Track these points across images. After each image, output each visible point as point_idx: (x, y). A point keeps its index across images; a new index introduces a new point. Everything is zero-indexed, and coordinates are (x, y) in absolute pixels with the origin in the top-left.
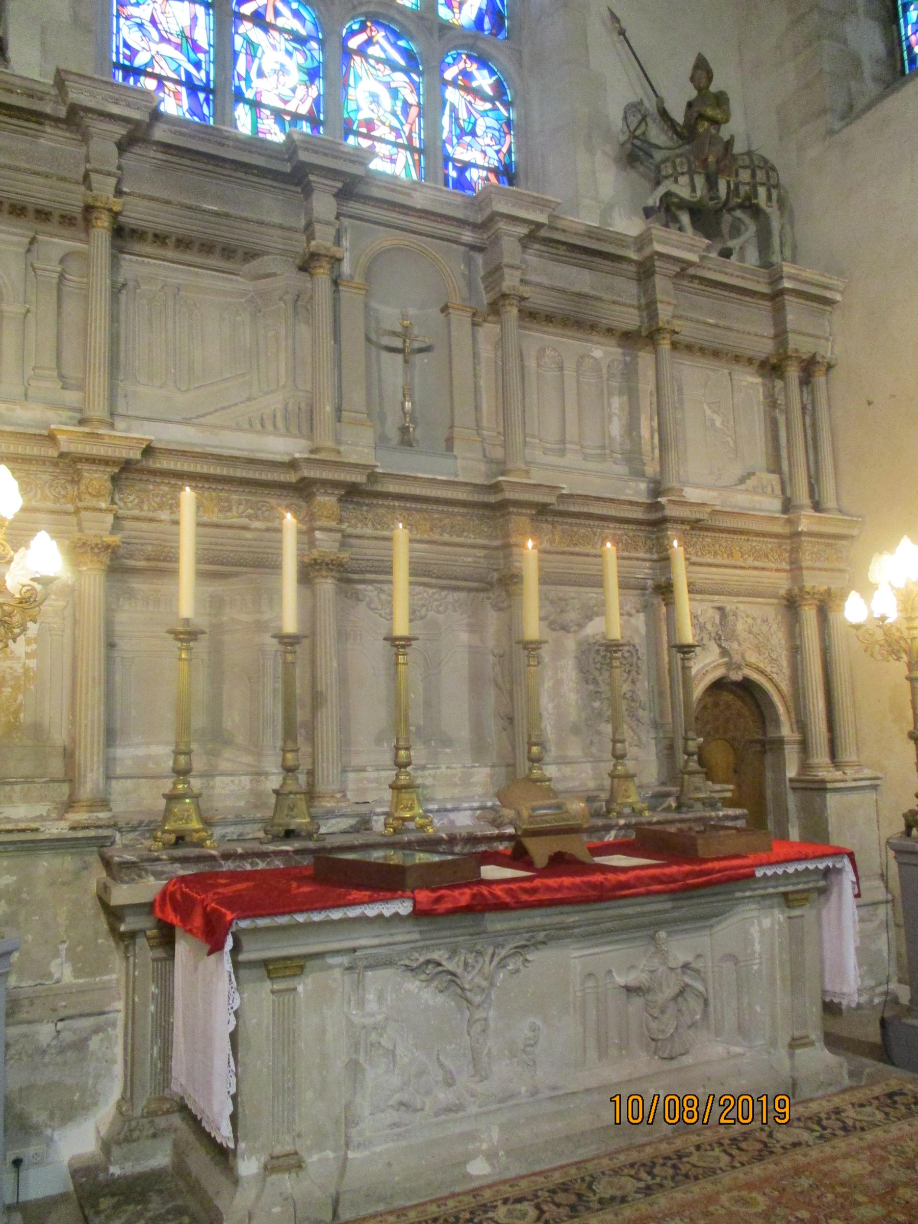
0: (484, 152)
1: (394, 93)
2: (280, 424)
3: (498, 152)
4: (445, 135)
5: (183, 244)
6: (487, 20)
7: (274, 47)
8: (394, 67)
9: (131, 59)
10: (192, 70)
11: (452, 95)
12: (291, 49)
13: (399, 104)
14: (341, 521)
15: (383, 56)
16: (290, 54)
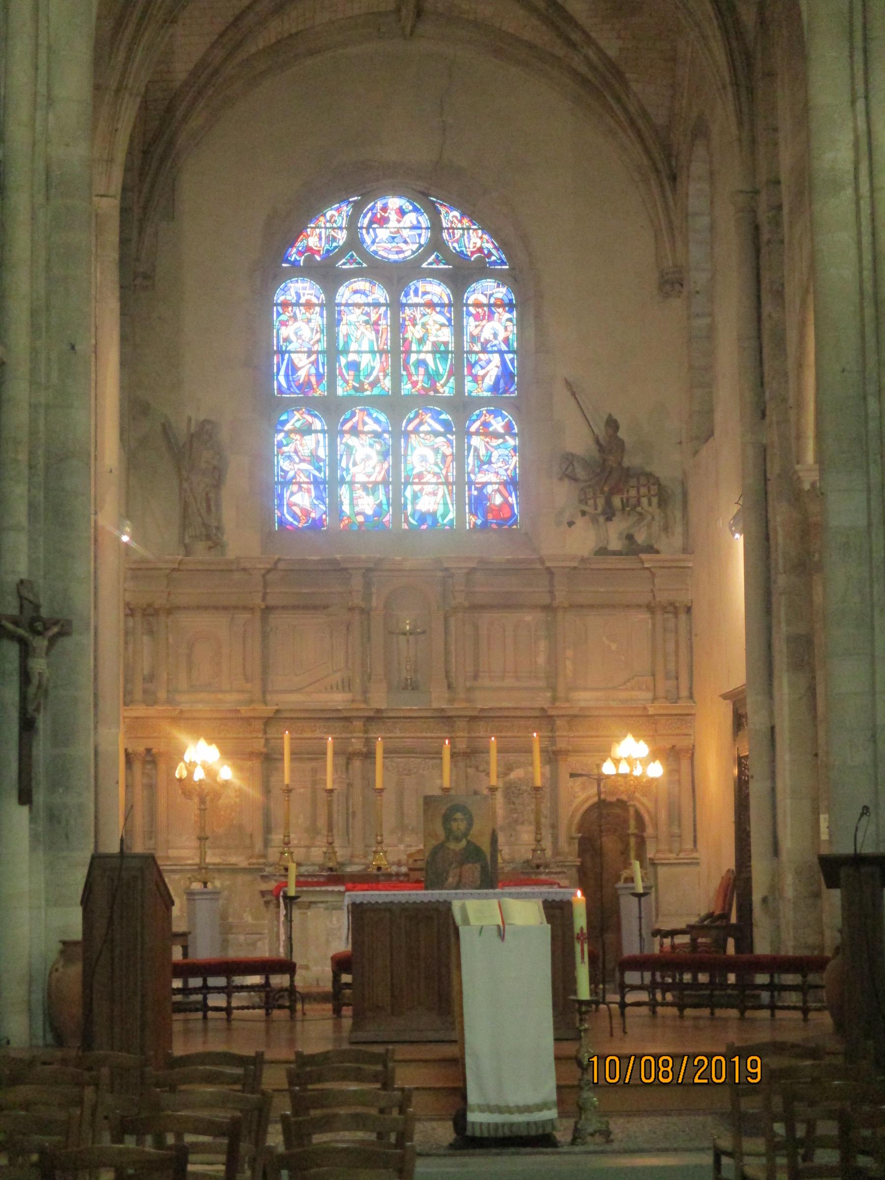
0: (497, 473)
1: (436, 450)
2: (340, 687)
3: (506, 470)
4: (470, 467)
5: (295, 607)
6: (502, 382)
7: (363, 445)
8: (436, 434)
9: (284, 477)
10: (317, 473)
11: (476, 441)
12: (372, 442)
13: (440, 456)
14: (366, 732)
15: (429, 429)
16: (371, 446)
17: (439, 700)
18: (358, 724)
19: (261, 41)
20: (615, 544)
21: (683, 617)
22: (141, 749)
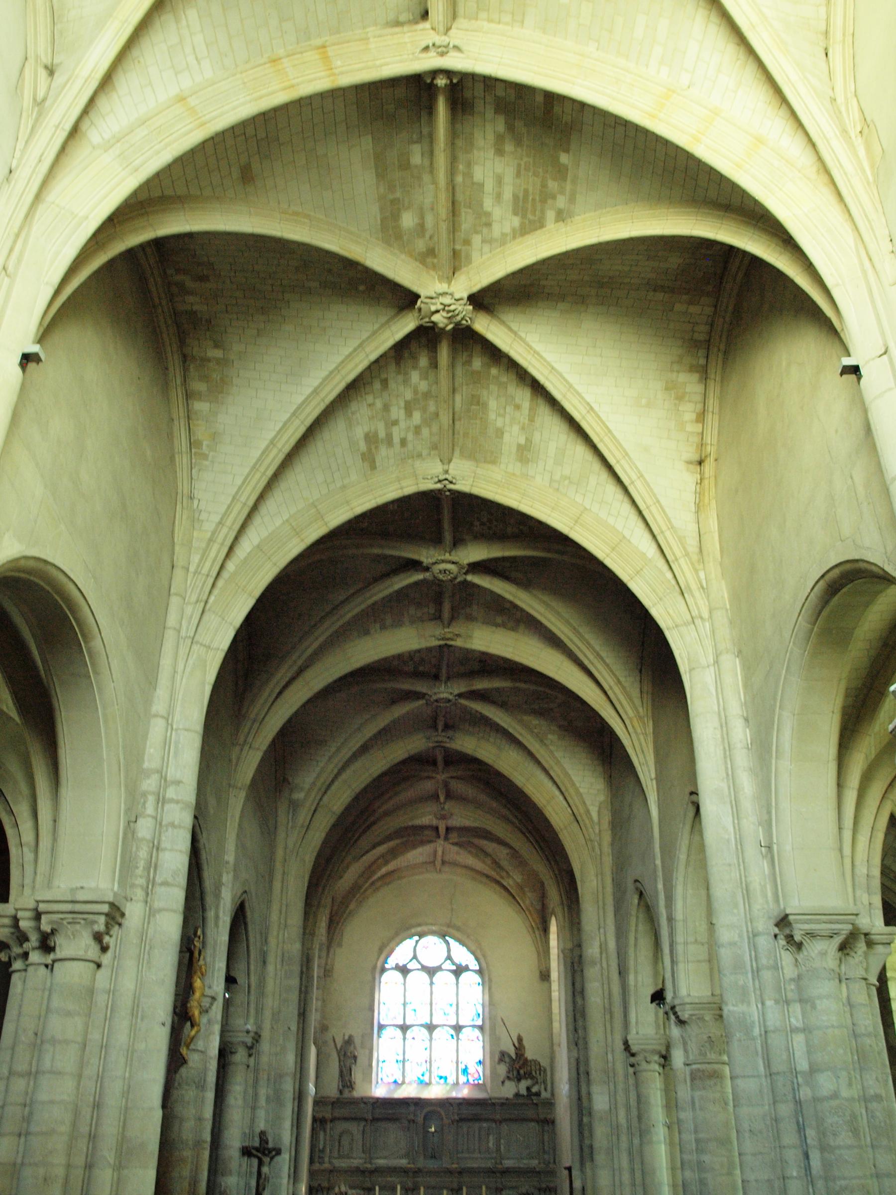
17: (446, 1163)
18: (411, 1174)
19: (379, 874)
20: (524, 1092)
21: (551, 1126)
22: (316, 1185)
